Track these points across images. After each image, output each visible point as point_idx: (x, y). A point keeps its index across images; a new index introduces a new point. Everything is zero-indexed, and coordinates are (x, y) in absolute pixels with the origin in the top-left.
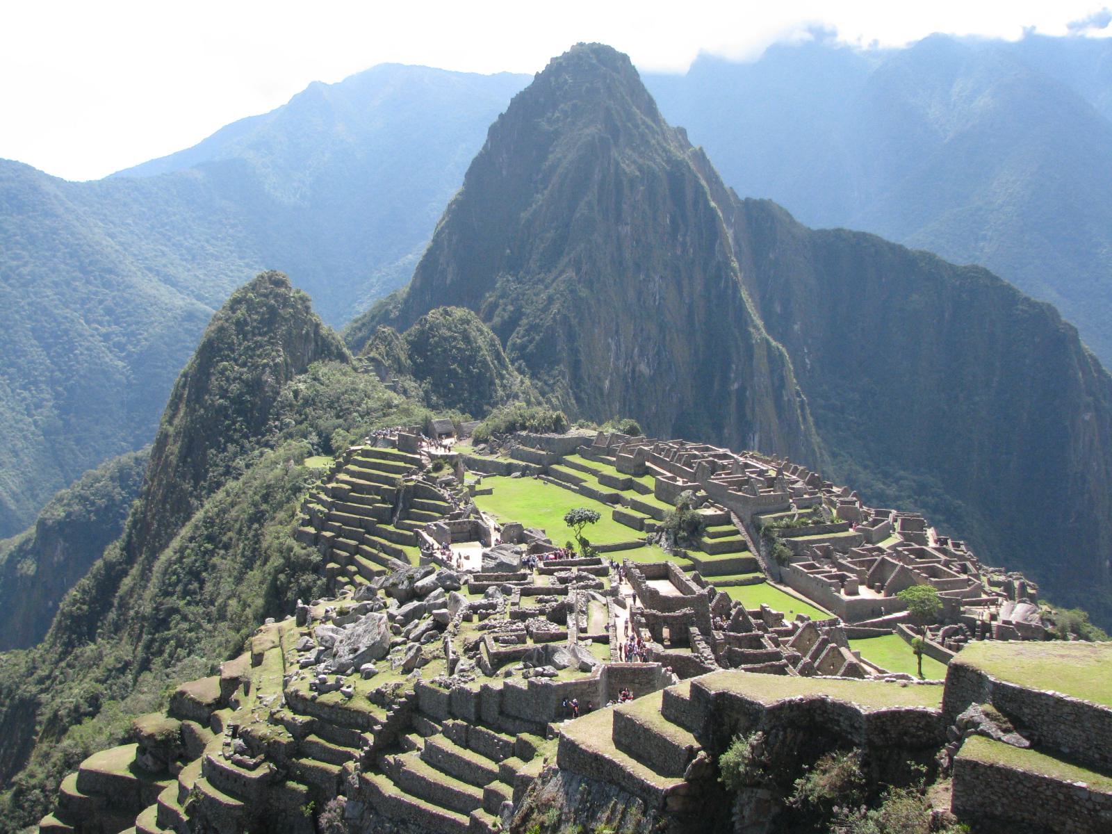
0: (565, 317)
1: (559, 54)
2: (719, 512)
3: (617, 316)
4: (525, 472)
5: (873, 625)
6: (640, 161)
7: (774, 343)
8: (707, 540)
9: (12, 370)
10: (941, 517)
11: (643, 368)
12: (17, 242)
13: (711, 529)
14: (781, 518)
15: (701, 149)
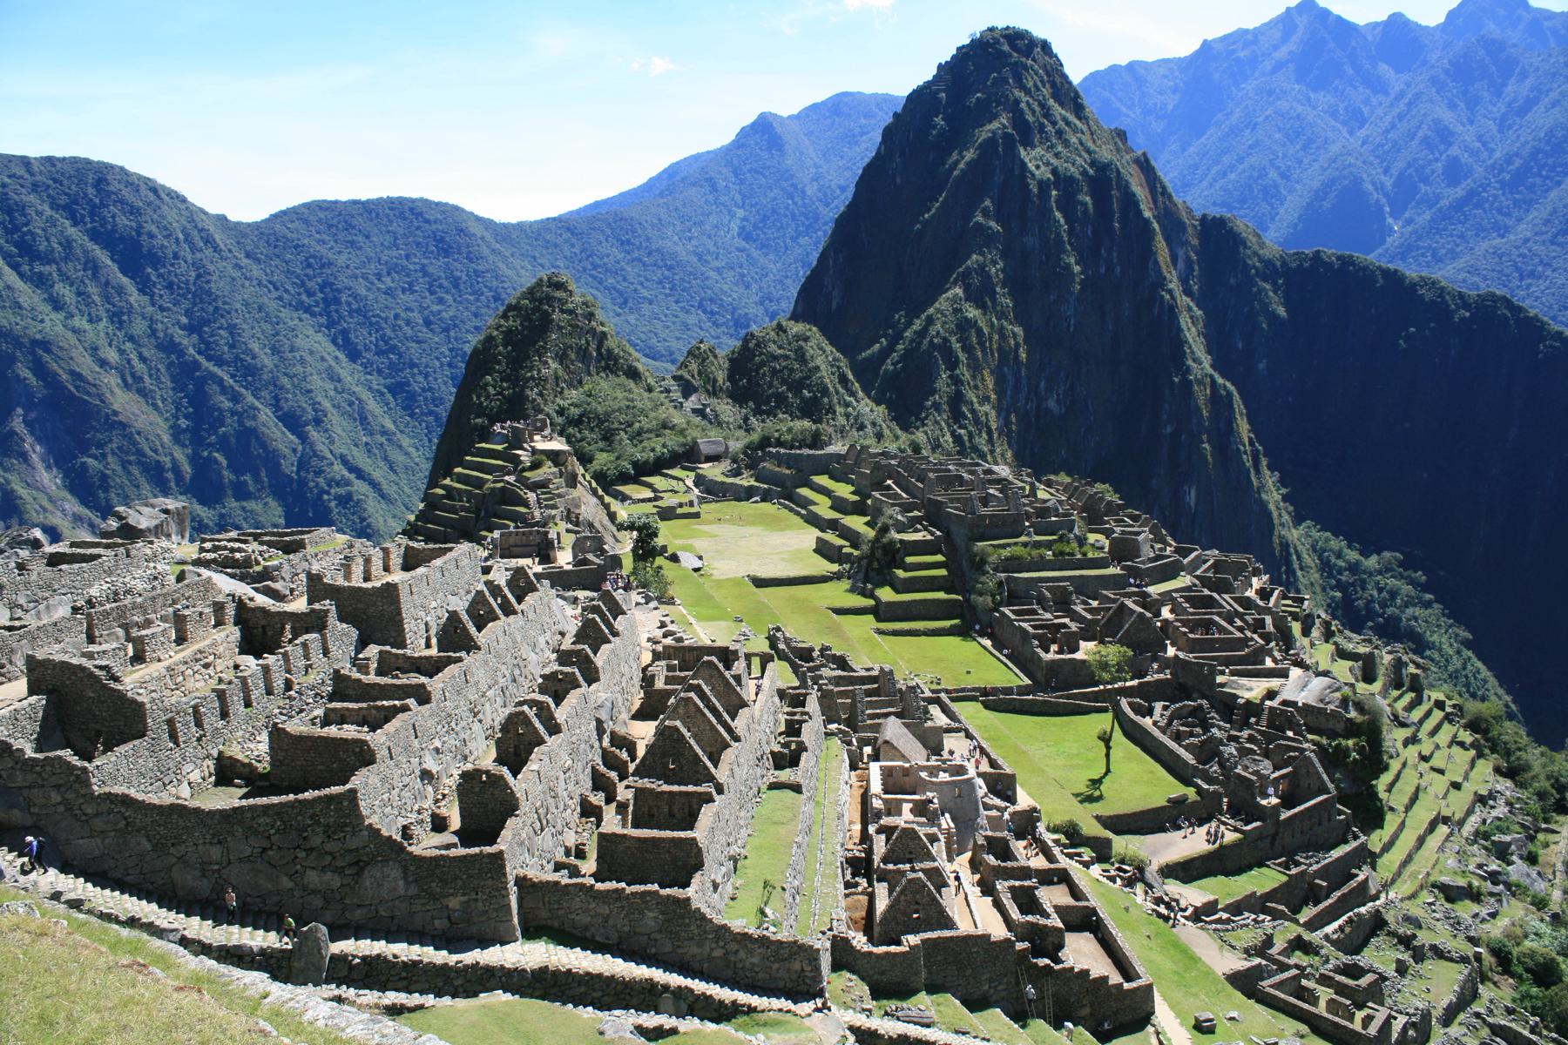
0: (945, 340)
1: (967, 41)
2: (929, 537)
3: (1017, 345)
4: (766, 497)
5: (1084, 697)
6: (1054, 161)
7: (1220, 381)
8: (900, 573)
9: (431, 419)
10: (1429, 596)
11: (1051, 404)
12: (441, 286)
13: (909, 560)
14: (1004, 546)
15: (1144, 154)
